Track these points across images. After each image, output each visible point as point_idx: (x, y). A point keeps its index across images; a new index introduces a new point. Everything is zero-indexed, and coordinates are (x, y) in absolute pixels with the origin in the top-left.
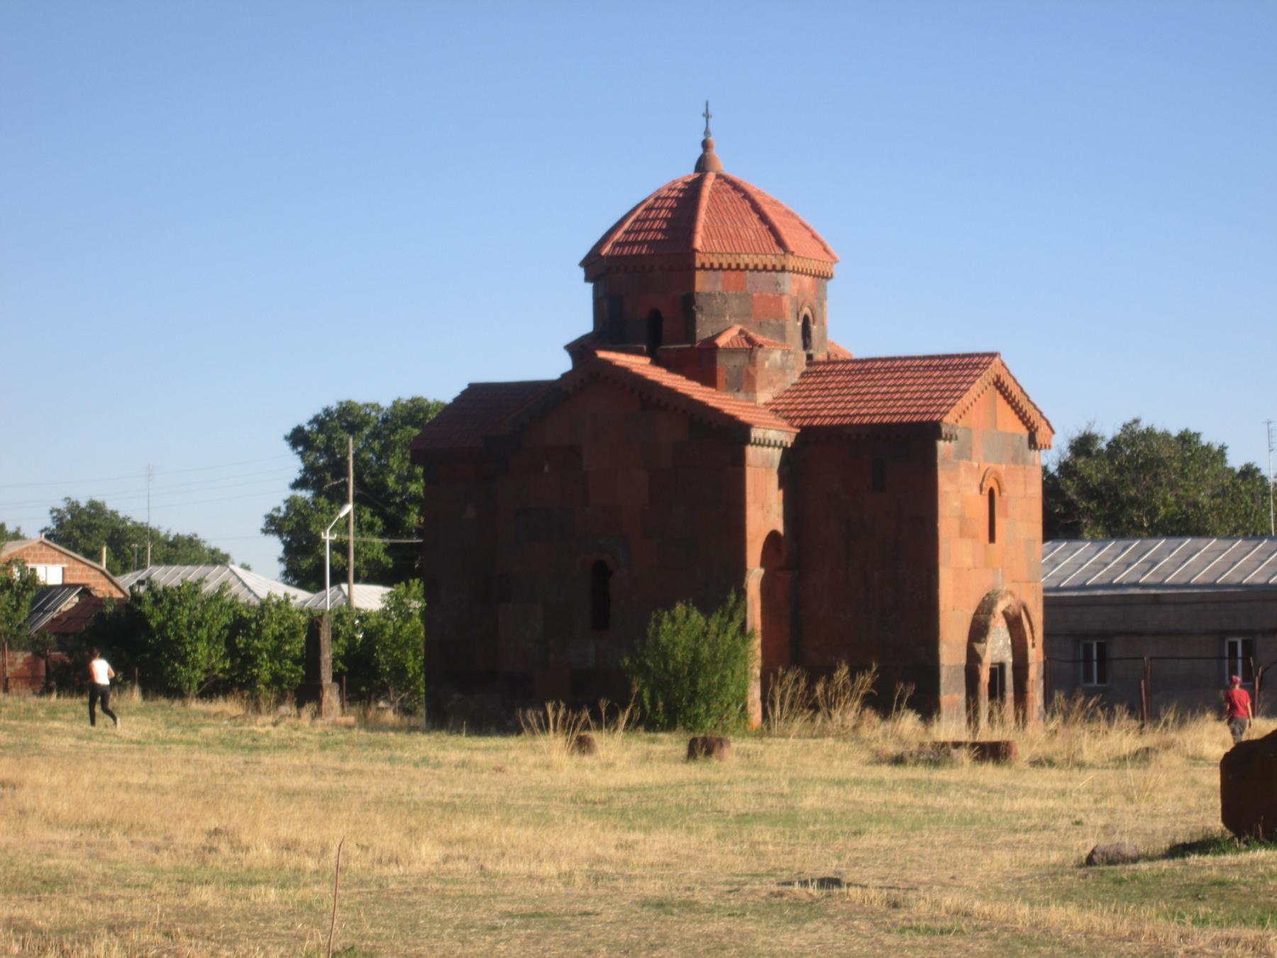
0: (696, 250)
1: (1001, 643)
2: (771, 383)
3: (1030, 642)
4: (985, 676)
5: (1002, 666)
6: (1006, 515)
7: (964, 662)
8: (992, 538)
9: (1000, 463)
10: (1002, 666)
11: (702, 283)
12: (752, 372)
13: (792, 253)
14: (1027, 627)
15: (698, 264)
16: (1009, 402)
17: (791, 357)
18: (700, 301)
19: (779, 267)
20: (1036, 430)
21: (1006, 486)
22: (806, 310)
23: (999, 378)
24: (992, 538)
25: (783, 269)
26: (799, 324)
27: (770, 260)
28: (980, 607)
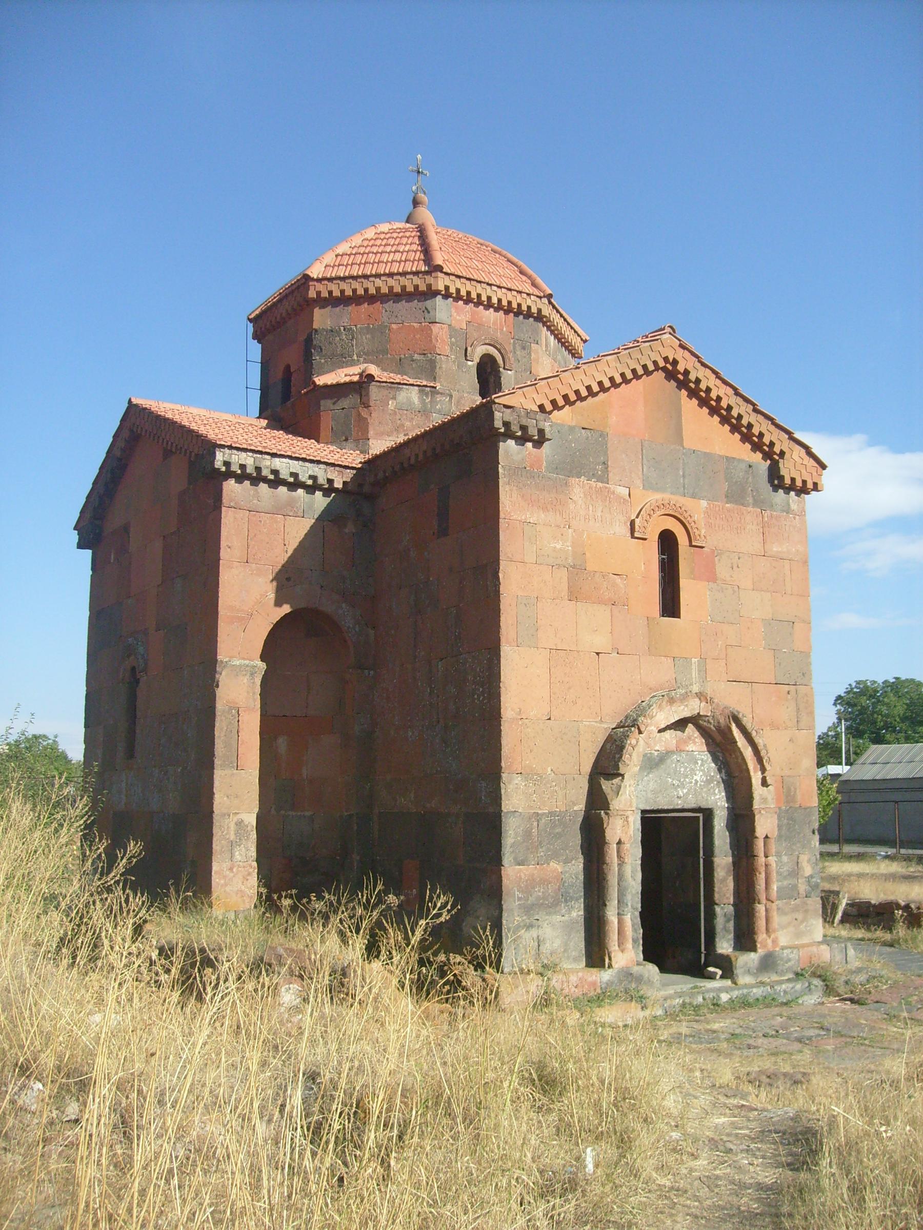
0: (306, 278)
1: (699, 777)
2: (398, 429)
3: (756, 778)
4: (624, 832)
5: (708, 813)
6: (712, 577)
7: (580, 807)
8: (671, 605)
9: (694, 496)
10: (708, 813)
11: (321, 318)
12: (364, 413)
13: (439, 268)
14: (748, 752)
15: (312, 294)
16: (714, 411)
17: (439, 398)
18: (317, 340)
19: (423, 288)
20: (782, 454)
21: (701, 530)
22: (481, 350)
23: (675, 362)
24: (671, 605)
25: (431, 293)
26: (472, 364)
27: (409, 283)
28: (627, 717)
